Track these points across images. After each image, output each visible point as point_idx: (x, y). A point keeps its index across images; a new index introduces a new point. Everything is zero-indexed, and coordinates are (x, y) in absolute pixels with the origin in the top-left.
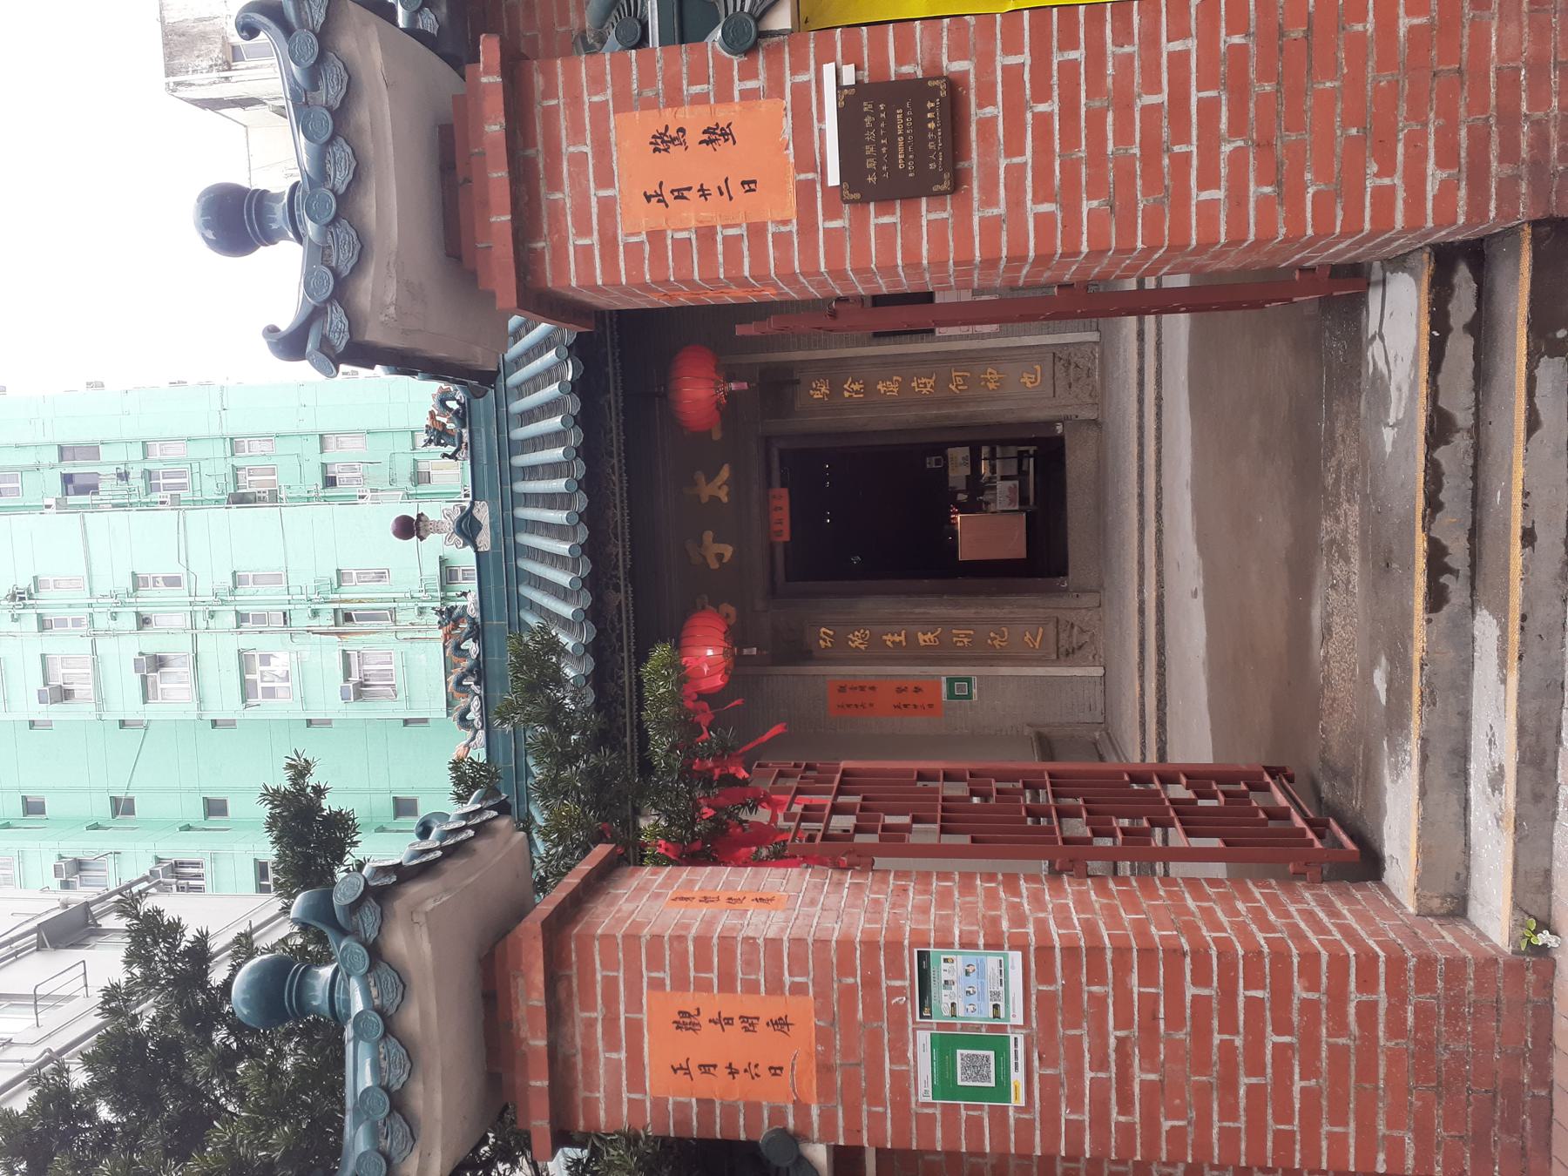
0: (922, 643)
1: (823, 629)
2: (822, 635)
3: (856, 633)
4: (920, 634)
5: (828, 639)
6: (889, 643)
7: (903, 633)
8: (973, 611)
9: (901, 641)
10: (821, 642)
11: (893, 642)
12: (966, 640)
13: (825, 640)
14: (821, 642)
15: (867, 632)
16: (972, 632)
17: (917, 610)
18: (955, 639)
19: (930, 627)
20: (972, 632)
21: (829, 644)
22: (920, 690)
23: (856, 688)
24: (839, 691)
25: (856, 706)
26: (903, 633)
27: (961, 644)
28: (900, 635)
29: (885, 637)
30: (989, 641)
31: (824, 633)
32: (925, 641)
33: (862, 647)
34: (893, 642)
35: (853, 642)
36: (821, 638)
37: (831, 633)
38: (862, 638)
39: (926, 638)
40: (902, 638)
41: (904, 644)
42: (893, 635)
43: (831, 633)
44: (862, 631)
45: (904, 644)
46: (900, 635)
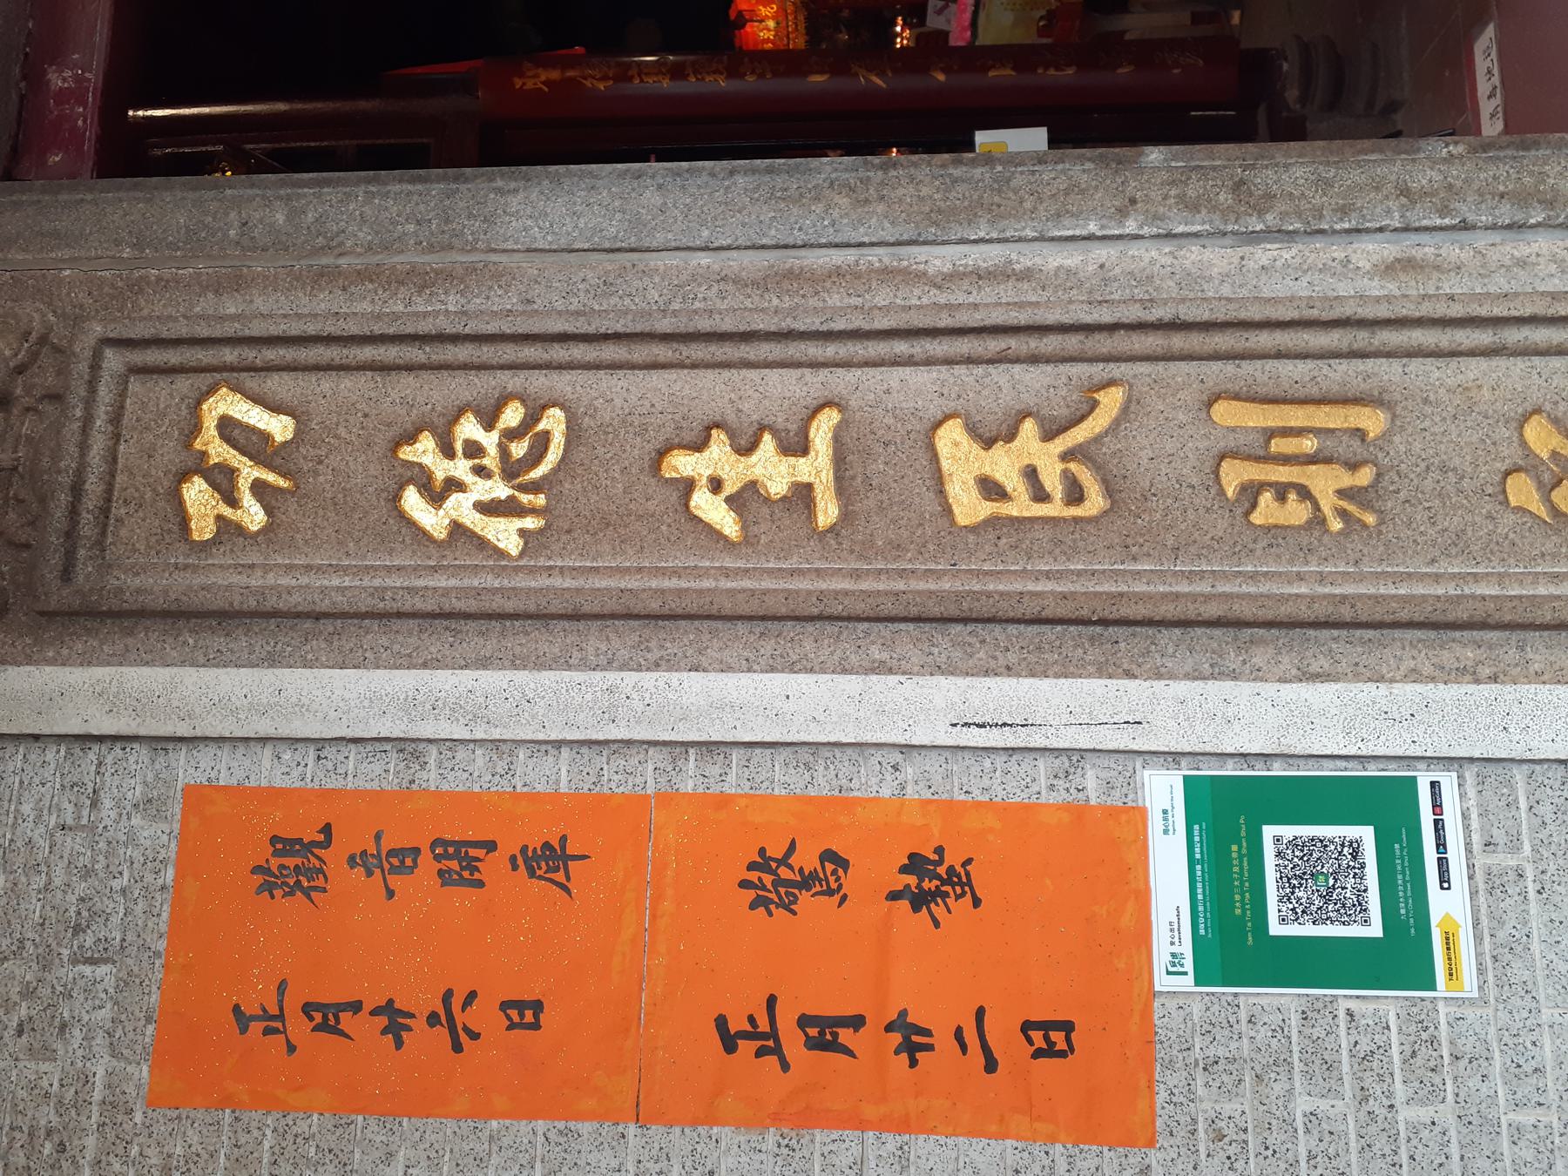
0: (969, 507)
1: (228, 404)
2: (218, 451)
3: (469, 428)
4: (951, 438)
5: (249, 472)
6: (711, 509)
7: (822, 431)
8: (1369, 251)
9: (803, 494)
10: (196, 493)
11: (746, 499)
12: (1325, 483)
13: (223, 482)
14: (196, 493)
15: (554, 422)
16: (1373, 421)
17: (939, 259)
18: (1234, 475)
19: (1032, 382)
20: (1373, 421)
21: (253, 515)
22: (959, 882)
23: (403, 859)
24: (270, 882)
25: (394, 1020)
26: (822, 431)
27: (1296, 512)
28: (796, 446)
29: (683, 464)
30: (1522, 491)
31: (228, 427)
32: (991, 489)
33: (505, 534)
34: (746, 499)
35: (437, 494)
36: (200, 466)
37: (279, 427)
38: (511, 470)
39: (1004, 465)
40: (817, 467)
41: (827, 511)
42: (746, 449)
43: (279, 427)
44: (512, 416)
45: (827, 511)
46: (796, 446)
